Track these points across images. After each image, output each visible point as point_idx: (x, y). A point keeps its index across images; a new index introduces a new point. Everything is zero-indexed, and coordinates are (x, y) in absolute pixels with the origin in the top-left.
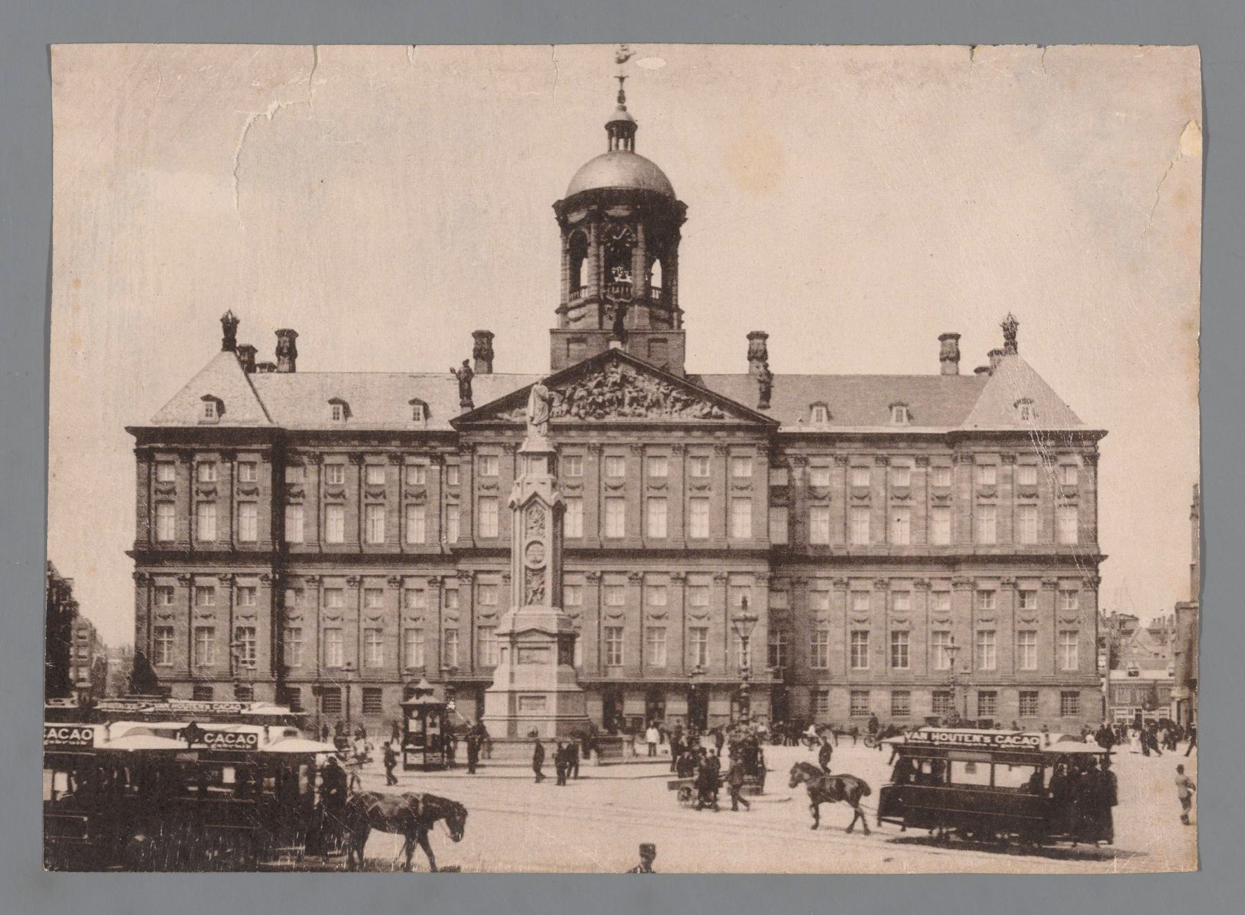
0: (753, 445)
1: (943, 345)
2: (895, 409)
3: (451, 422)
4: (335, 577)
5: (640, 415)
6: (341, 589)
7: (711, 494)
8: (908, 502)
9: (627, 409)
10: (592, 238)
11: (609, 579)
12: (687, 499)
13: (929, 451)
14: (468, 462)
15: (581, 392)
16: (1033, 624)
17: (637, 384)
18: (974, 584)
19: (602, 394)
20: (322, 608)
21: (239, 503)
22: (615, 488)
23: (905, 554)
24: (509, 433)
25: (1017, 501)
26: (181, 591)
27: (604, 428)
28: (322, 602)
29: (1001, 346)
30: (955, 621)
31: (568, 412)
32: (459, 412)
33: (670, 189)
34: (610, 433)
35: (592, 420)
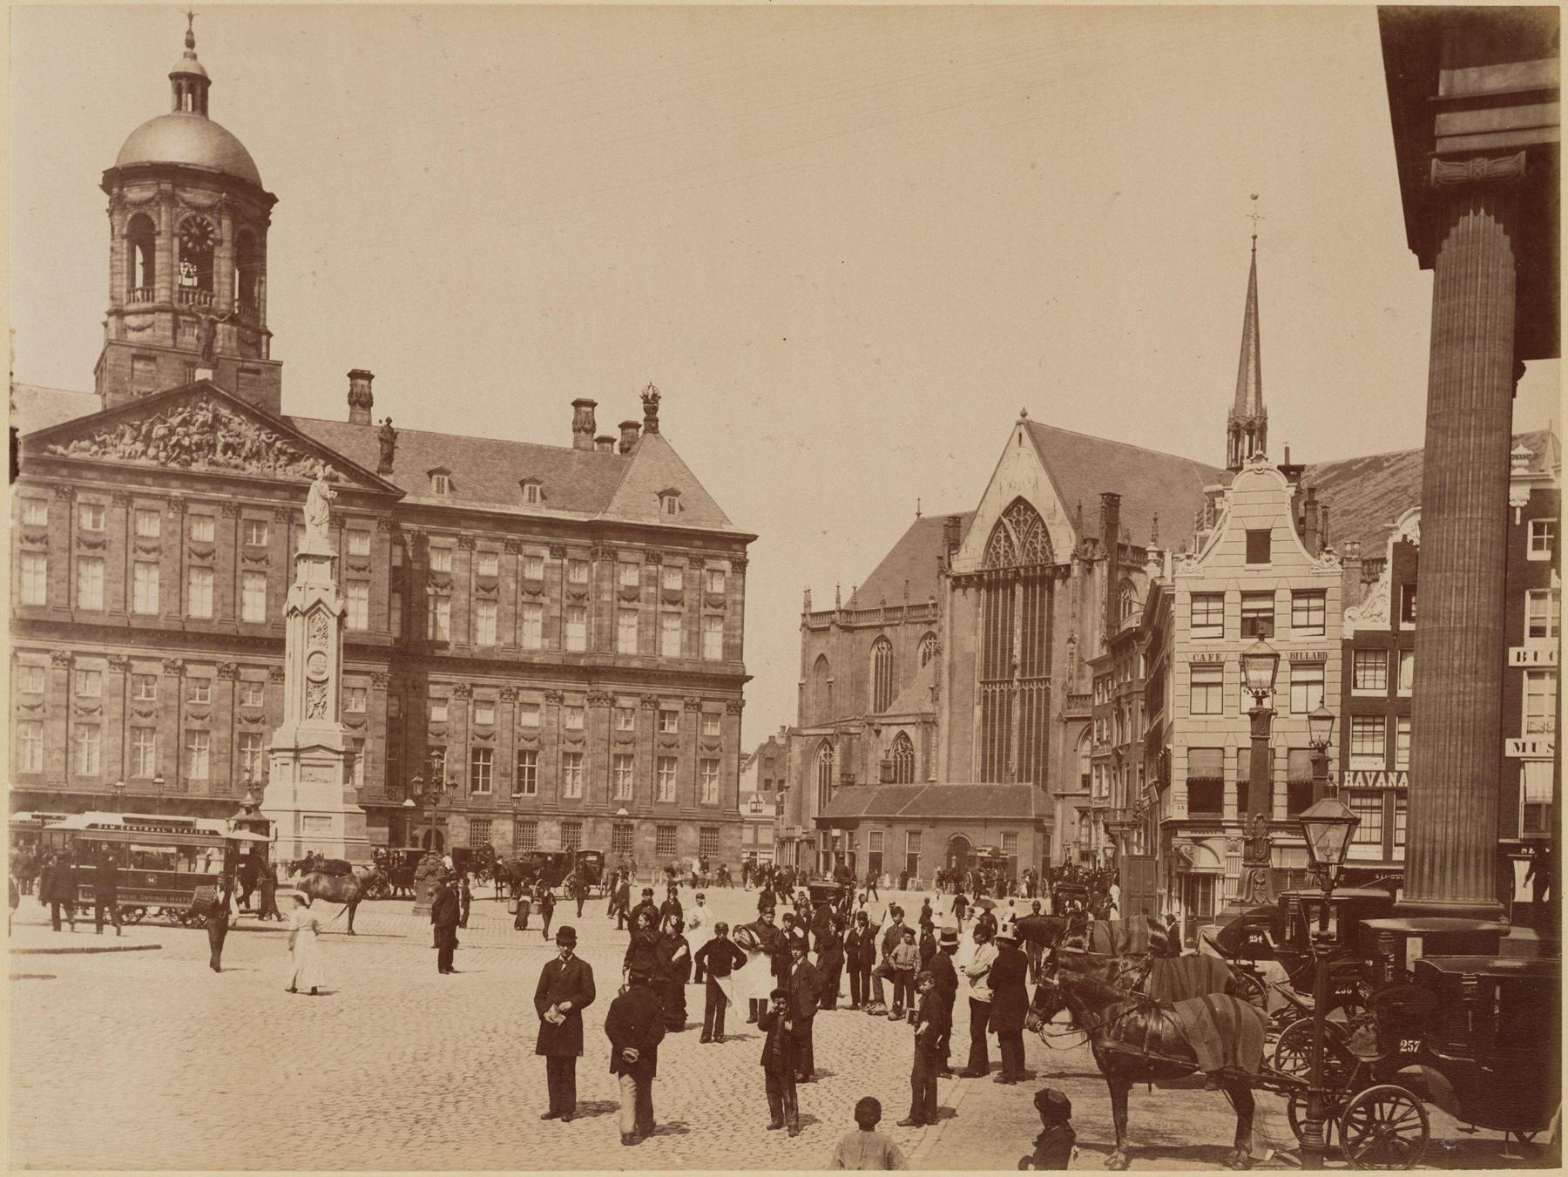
0: (374, 518)
1: (577, 412)
5: (236, 467)
8: (541, 599)
10: (163, 228)
15: (160, 430)
17: (232, 426)
18: (657, 704)
19: (187, 435)
30: (589, 743)
31: (144, 453)
35: (173, 465)
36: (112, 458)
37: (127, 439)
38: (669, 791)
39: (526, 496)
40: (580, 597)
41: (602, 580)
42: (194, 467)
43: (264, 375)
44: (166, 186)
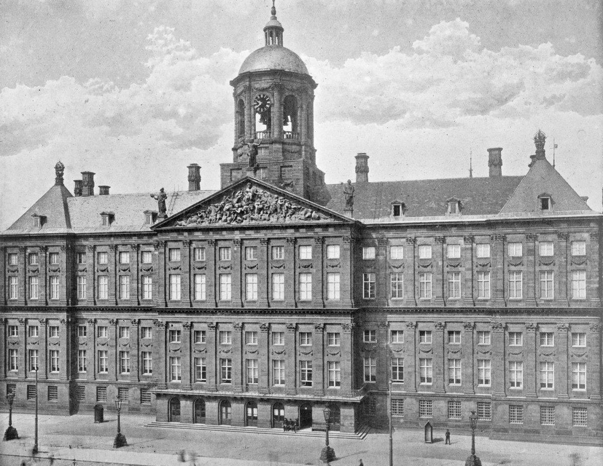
3: (151, 228)
4: (104, 319)
5: (265, 220)
7: (313, 270)
9: (256, 216)
12: (297, 273)
17: (263, 198)
19: (242, 206)
22: (252, 268)
27: (243, 229)
31: (220, 219)
34: (248, 232)
35: (234, 224)
36: (205, 224)
37: (213, 214)
42: (245, 223)
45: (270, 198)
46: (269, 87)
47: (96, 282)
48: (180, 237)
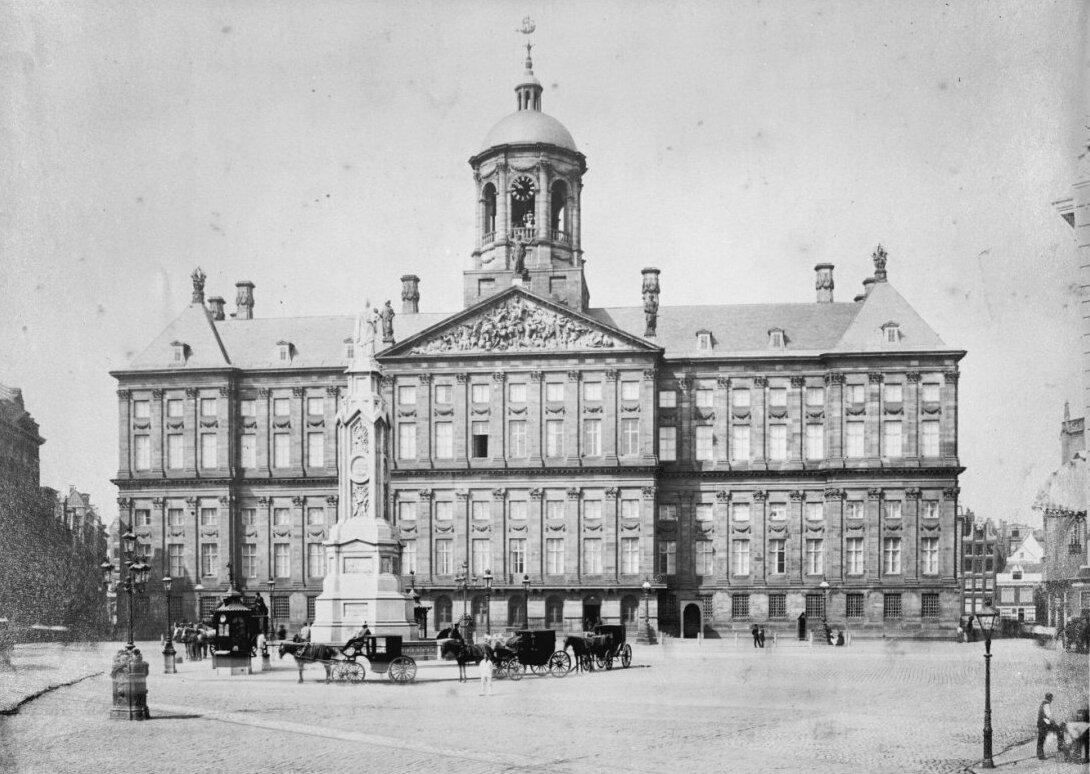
0: (640, 370)
2: (772, 334)
4: (283, 497)
6: (288, 509)
9: (526, 340)
11: (513, 495)
13: (805, 372)
14: (390, 392)
16: (897, 531)
17: (536, 316)
19: (506, 328)
20: (272, 526)
21: (202, 434)
22: (518, 412)
23: (783, 468)
24: (425, 365)
25: (883, 418)
26: (156, 513)
28: (273, 520)
29: (872, 275)
30: (827, 529)
31: (476, 344)
32: (382, 347)
33: (572, 143)
34: (513, 363)
35: (496, 351)
36: (455, 351)
37: (465, 336)
38: (897, 566)
39: (772, 342)
40: (816, 416)
41: (832, 401)
42: (511, 350)
43: (568, 279)
44: (501, 159)
45: (545, 317)
46: (534, 167)
47: (271, 442)
48: (417, 370)
